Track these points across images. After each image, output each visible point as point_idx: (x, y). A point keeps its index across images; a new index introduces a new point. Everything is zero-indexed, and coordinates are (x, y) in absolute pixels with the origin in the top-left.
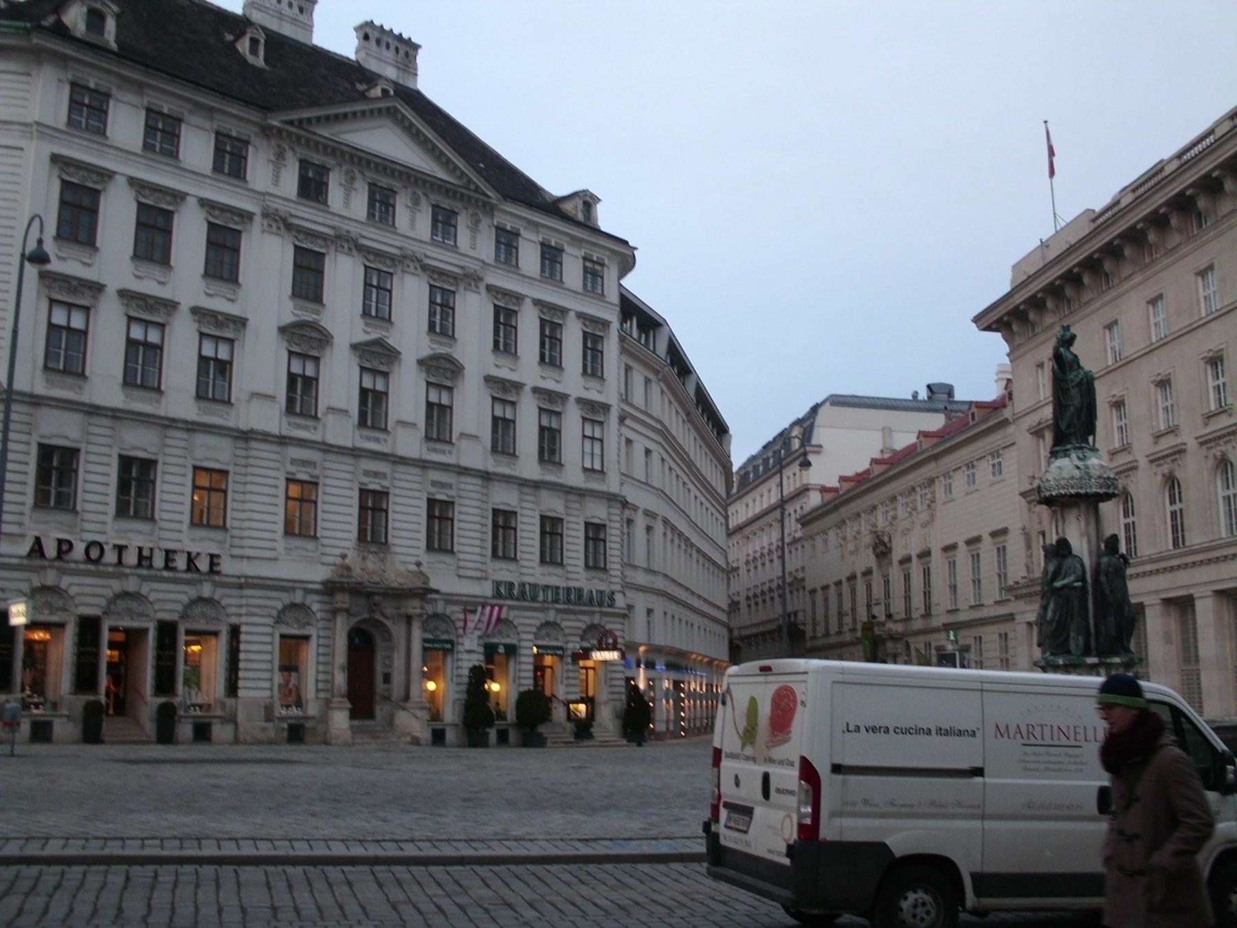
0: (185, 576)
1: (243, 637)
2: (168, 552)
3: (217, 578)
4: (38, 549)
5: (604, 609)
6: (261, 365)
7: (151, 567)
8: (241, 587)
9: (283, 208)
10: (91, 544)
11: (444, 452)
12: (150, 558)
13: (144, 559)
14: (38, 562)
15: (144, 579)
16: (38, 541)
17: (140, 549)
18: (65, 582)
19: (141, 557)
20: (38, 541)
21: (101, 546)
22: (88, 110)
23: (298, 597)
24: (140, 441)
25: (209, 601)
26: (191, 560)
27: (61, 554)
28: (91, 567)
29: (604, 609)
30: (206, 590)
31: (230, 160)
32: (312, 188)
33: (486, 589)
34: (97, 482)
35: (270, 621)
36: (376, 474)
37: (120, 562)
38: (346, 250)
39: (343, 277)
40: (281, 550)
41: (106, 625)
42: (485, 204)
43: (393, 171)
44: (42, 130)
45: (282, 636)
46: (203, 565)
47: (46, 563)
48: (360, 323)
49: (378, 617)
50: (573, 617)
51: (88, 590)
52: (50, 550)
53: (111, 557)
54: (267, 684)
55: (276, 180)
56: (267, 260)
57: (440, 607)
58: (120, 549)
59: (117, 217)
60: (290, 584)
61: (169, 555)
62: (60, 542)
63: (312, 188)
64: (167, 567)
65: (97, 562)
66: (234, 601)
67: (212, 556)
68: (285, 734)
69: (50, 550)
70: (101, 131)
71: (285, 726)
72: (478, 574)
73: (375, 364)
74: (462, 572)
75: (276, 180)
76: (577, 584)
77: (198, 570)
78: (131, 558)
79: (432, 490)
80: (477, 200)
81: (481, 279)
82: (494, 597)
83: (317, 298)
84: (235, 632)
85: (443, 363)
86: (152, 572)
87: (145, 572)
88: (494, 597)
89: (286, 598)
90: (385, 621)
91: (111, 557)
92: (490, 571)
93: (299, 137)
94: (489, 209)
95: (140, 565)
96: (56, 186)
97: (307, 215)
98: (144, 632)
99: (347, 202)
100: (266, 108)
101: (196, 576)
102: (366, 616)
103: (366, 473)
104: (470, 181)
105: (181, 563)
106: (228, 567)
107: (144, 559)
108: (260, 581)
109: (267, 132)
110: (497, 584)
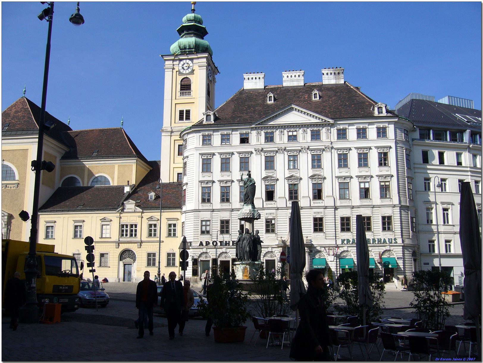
4: (201, 244)
12: (229, 244)
14: (201, 247)
15: (228, 248)
16: (201, 242)
20: (201, 242)
22: (207, 140)
23: (270, 249)
24: (225, 216)
27: (207, 245)
32: (269, 139)
33: (339, 242)
34: (216, 227)
42: (329, 124)
43: (294, 126)
44: (196, 149)
48: (287, 171)
50: (377, 248)
52: (204, 244)
59: (216, 163)
62: (206, 242)
63: (269, 139)
69: (204, 244)
70: (210, 144)
74: (327, 238)
79: (315, 215)
80: (326, 124)
93: (262, 127)
94: (332, 125)
96: (201, 160)
97: (269, 146)
98: (229, 261)
99: (281, 139)
100: (251, 123)
104: (322, 119)
109: (252, 129)
110: (343, 241)
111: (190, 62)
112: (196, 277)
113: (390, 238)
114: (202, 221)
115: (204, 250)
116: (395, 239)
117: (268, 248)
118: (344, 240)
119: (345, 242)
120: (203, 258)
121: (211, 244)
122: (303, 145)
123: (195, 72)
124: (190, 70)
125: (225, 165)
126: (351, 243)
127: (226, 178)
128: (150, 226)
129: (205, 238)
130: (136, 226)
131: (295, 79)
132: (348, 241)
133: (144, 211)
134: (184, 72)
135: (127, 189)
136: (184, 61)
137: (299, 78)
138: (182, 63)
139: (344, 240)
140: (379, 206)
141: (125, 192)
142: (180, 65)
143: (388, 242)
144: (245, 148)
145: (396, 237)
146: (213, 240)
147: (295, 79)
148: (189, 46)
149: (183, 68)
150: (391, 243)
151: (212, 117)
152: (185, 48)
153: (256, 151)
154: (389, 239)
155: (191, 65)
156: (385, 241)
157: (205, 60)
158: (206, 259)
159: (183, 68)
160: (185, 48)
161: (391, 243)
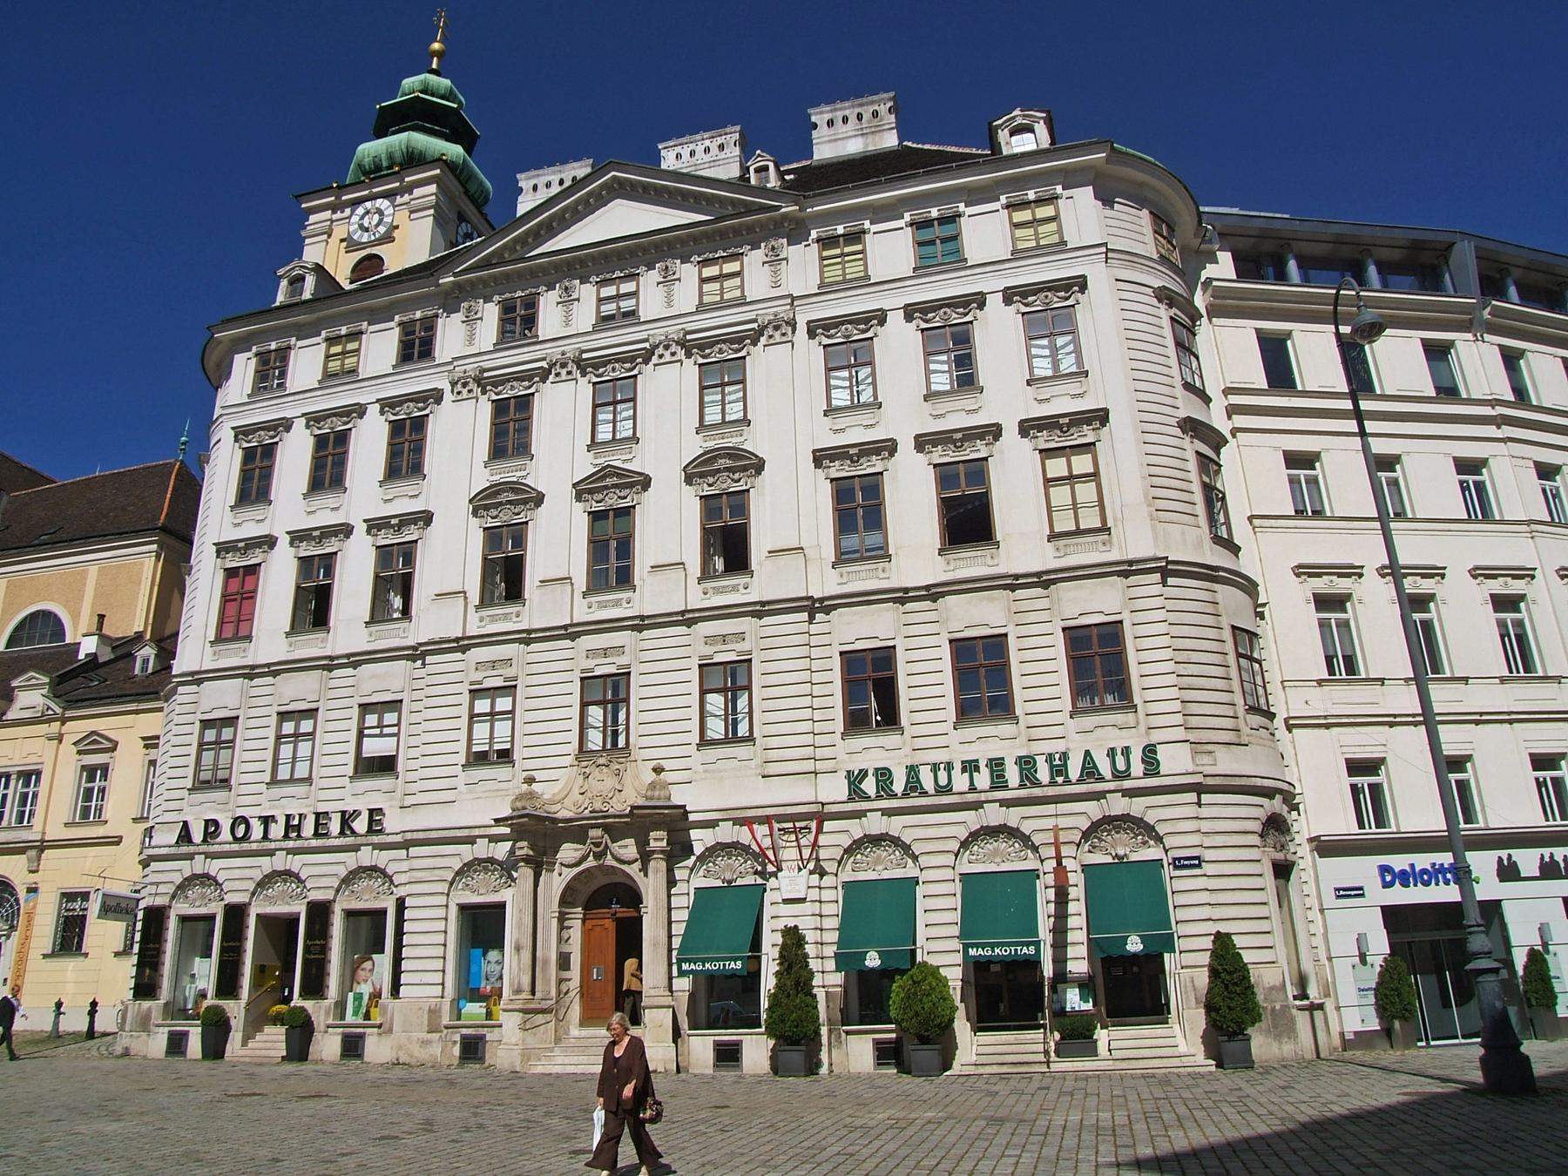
0: (314, 843)
1: (407, 914)
2: (318, 815)
3: (375, 839)
4: (185, 836)
5: (1127, 784)
6: (451, 557)
7: (299, 836)
8: (406, 845)
9: (471, 367)
10: (238, 820)
11: (735, 588)
12: (298, 828)
13: (292, 828)
14: (185, 849)
17: (288, 817)
18: (214, 867)
19: (288, 827)
20: (185, 823)
21: (245, 820)
23: (482, 849)
25: (374, 869)
26: (347, 819)
27: (205, 841)
28: (235, 847)
29: (1127, 784)
30: (366, 857)
31: (417, 348)
32: (519, 323)
33: (834, 790)
35: (444, 887)
36: (605, 652)
37: (265, 837)
38: (564, 376)
39: (562, 412)
40: (462, 788)
41: (253, 912)
45: (463, 908)
46: (360, 825)
47: (192, 849)
49: (609, 861)
50: (1050, 809)
51: (237, 873)
52: (197, 835)
53: (257, 831)
54: (438, 978)
55: (471, 339)
56: (459, 434)
57: (726, 833)
58: (267, 821)
60: (465, 833)
61: (321, 818)
64: (317, 835)
65: (246, 838)
66: (404, 866)
67: (371, 811)
68: (457, 1050)
69: (197, 836)
71: (457, 1038)
72: (808, 766)
73: (612, 501)
75: (471, 339)
76: (1057, 747)
77: (353, 832)
78: (277, 830)
81: (793, 324)
82: (850, 800)
83: (523, 449)
84: (401, 905)
85: (724, 463)
86: (299, 843)
87: (291, 844)
88: (850, 800)
89: (467, 852)
90: (624, 867)
91: (257, 831)
92: (842, 756)
95: (286, 836)
101: (350, 840)
102: (591, 862)
103: (591, 653)
105: (335, 826)
106: (394, 823)
107: (293, 828)
108: (421, 835)
110: (855, 781)
111: (383, 203)
112: (146, 1004)
113: (1119, 745)
114: (206, 724)
115: (199, 865)
116: (1150, 752)
117: (471, 841)
118: (863, 774)
119: (869, 785)
120: (181, 908)
121: (226, 835)
122: (658, 333)
123: (396, 234)
124: (382, 229)
125: (328, 472)
126: (898, 787)
127: (326, 519)
128: (91, 772)
129: (215, 807)
130: (38, 773)
131: (707, 158)
132: (884, 775)
133: (69, 714)
134: (364, 240)
135: (89, 646)
136: (368, 204)
137: (722, 155)
138: (360, 211)
139: (863, 774)
140: (1043, 580)
141: (81, 656)
142: (355, 219)
143: (1106, 771)
144: (418, 381)
145: (1156, 736)
146: (240, 812)
147: (707, 158)
148: (390, 157)
149: (361, 227)
150: (1125, 775)
151: (310, 281)
152: (378, 168)
153: (453, 384)
154: (1112, 753)
155: (391, 210)
156: (1090, 770)
157: (433, 188)
158: (203, 911)
159: (361, 227)
160: (378, 168)
161: (1125, 775)
